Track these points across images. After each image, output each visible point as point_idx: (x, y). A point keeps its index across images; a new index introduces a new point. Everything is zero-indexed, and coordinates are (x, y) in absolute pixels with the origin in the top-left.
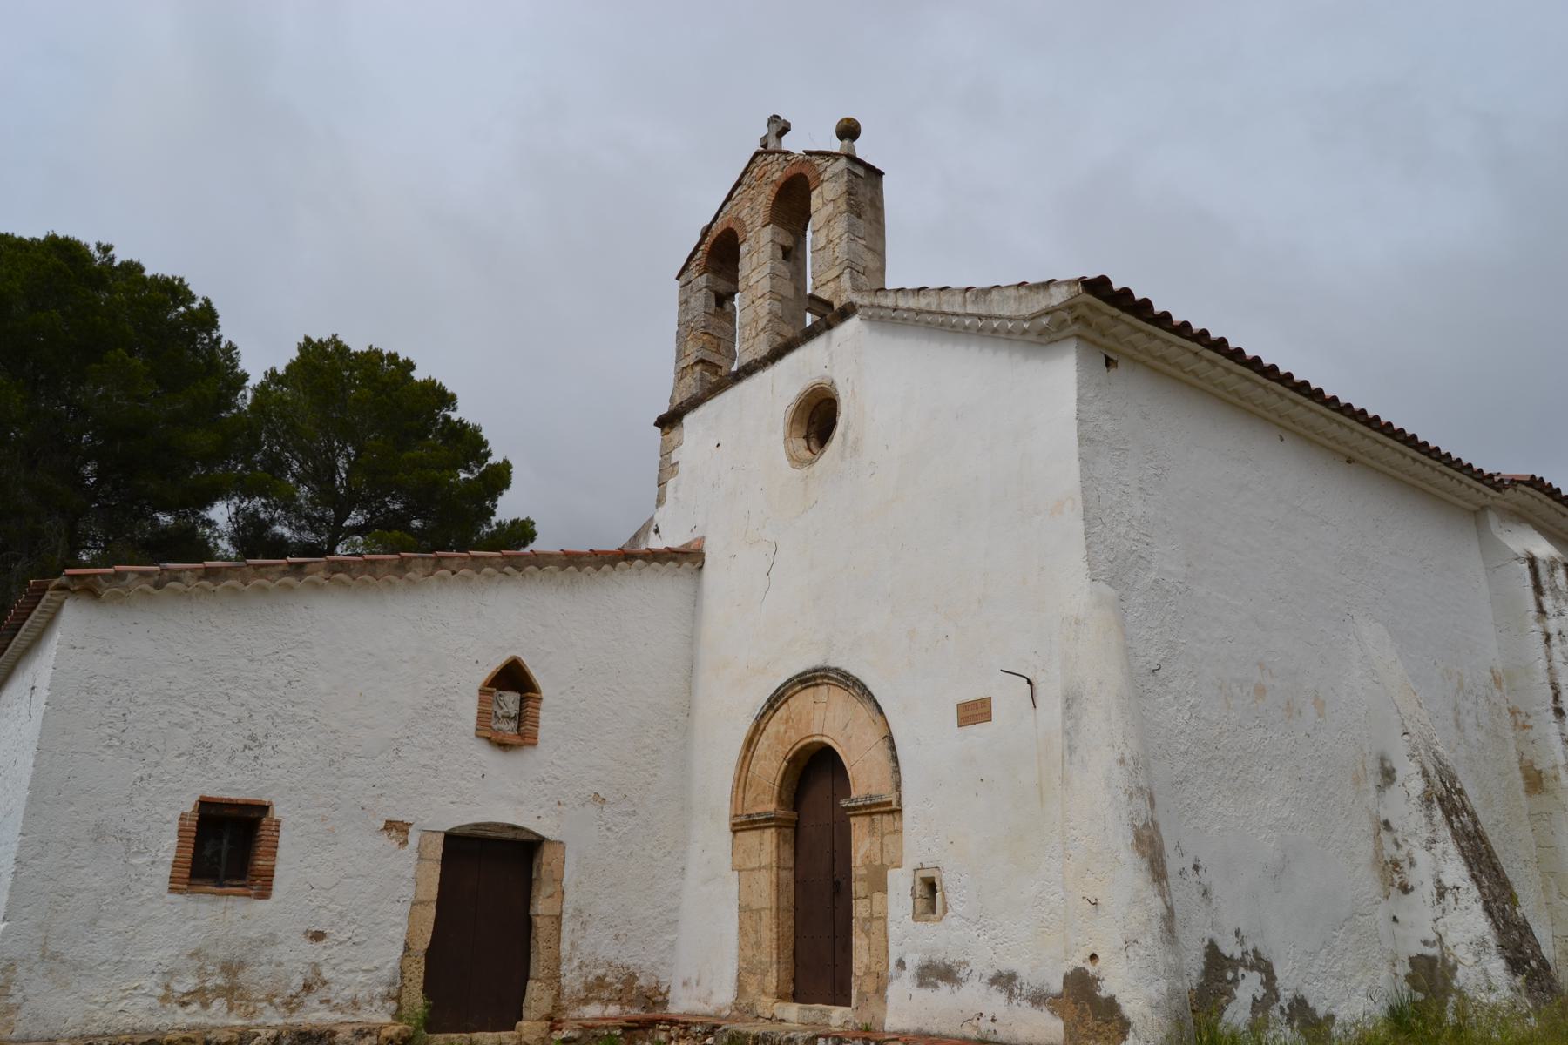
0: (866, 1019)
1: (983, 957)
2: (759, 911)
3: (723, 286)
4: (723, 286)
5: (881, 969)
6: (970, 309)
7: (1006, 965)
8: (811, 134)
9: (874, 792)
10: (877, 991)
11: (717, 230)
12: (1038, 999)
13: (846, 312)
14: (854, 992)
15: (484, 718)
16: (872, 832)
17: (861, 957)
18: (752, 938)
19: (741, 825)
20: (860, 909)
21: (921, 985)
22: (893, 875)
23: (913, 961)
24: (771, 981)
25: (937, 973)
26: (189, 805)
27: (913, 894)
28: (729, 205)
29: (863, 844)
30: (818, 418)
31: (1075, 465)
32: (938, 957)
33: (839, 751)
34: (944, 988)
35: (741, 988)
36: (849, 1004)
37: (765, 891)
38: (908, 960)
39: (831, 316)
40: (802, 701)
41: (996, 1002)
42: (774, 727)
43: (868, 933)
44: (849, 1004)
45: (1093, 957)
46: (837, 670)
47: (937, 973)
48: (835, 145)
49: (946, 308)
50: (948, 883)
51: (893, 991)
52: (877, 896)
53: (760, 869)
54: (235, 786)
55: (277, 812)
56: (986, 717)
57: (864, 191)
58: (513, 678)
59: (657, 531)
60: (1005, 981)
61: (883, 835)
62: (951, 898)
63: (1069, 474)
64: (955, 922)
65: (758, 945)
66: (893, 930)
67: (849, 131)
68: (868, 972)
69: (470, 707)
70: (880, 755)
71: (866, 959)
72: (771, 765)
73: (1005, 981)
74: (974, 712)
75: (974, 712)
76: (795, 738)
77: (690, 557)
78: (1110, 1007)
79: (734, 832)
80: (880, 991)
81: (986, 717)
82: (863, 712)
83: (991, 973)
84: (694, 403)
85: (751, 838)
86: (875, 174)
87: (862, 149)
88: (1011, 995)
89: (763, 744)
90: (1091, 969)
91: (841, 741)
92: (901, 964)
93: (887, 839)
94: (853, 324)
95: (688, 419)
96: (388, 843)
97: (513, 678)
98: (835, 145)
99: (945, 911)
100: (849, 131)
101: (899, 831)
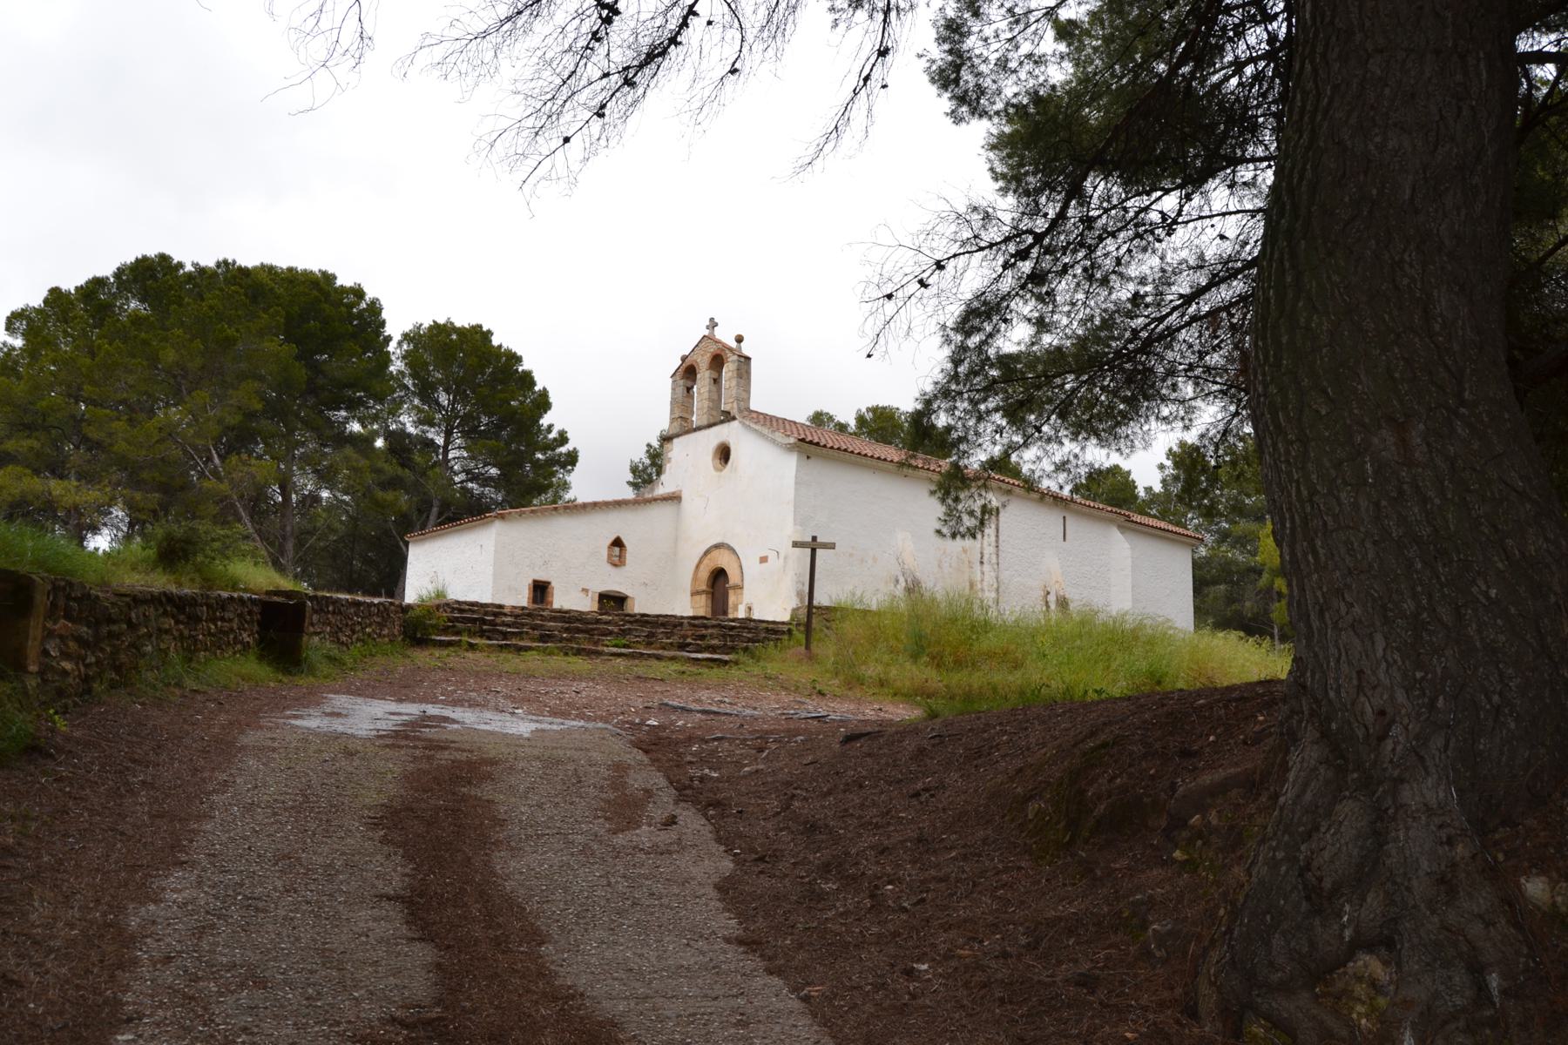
3: (689, 384)
4: (689, 384)
8: (726, 336)
11: (688, 362)
13: (734, 418)
15: (610, 556)
19: (694, 593)
26: (530, 581)
29: (732, 599)
31: (792, 492)
39: (728, 417)
40: (715, 553)
42: (706, 561)
48: (734, 344)
54: (542, 577)
55: (553, 584)
57: (744, 367)
58: (618, 543)
63: (790, 493)
67: (739, 339)
69: (605, 553)
70: (737, 571)
72: (705, 574)
74: (764, 560)
75: (764, 560)
77: (674, 498)
84: (678, 436)
85: (697, 598)
86: (748, 359)
87: (746, 349)
94: (735, 424)
96: (582, 595)
97: (618, 543)
98: (734, 344)
100: (739, 339)
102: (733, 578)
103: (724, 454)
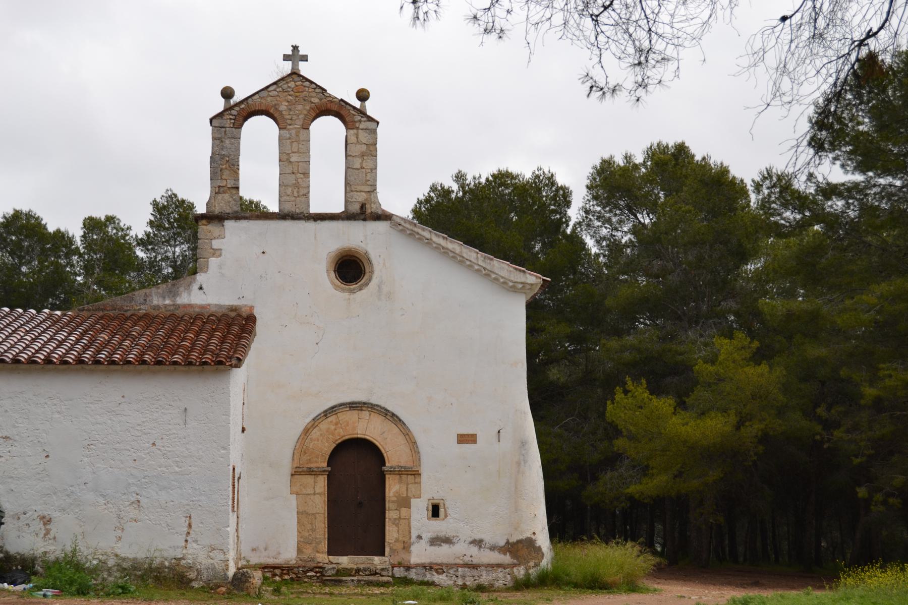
0: (395, 561)
1: (466, 532)
2: (314, 514)
5: (406, 540)
6: (481, 263)
7: (478, 537)
9: (402, 464)
10: (404, 548)
12: (493, 548)
14: (387, 550)
16: (400, 482)
17: (391, 533)
18: (309, 527)
19: (297, 472)
20: (390, 515)
21: (431, 545)
22: (413, 501)
23: (426, 536)
24: (324, 546)
25: (437, 541)
27: (427, 510)
28: (264, 94)
29: (393, 488)
30: (350, 269)
32: (442, 534)
33: (377, 443)
34: (445, 547)
35: (299, 551)
36: (382, 554)
37: (319, 505)
38: (424, 536)
41: (474, 550)
43: (397, 525)
44: (382, 554)
45: (534, 533)
46: (377, 406)
47: (437, 541)
49: (465, 255)
50: (451, 507)
51: (413, 548)
52: (404, 511)
53: (314, 494)
56: (475, 442)
59: (201, 288)
60: (478, 543)
61: (408, 484)
62: (449, 511)
64: (451, 521)
65: (313, 530)
66: (414, 524)
67: (363, 95)
68: (397, 540)
71: (395, 535)
73: (478, 543)
74: (466, 439)
75: (466, 439)
76: (342, 433)
78: (539, 548)
79: (292, 475)
80: (407, 547)
81: (475, 442)
82: (396, 430)
83: (471, 540)
85: (309, 479)
88: (480, 547)
89: (315, 433)
90: (533, 537)
91: (379, 439)
92: (420, 537)
93: (410, 486)
95: (229, 224)
99: (446, 516)
100: (363, 95)
101: (420, 483)
102: (394, 452)
103: (350, 269)
